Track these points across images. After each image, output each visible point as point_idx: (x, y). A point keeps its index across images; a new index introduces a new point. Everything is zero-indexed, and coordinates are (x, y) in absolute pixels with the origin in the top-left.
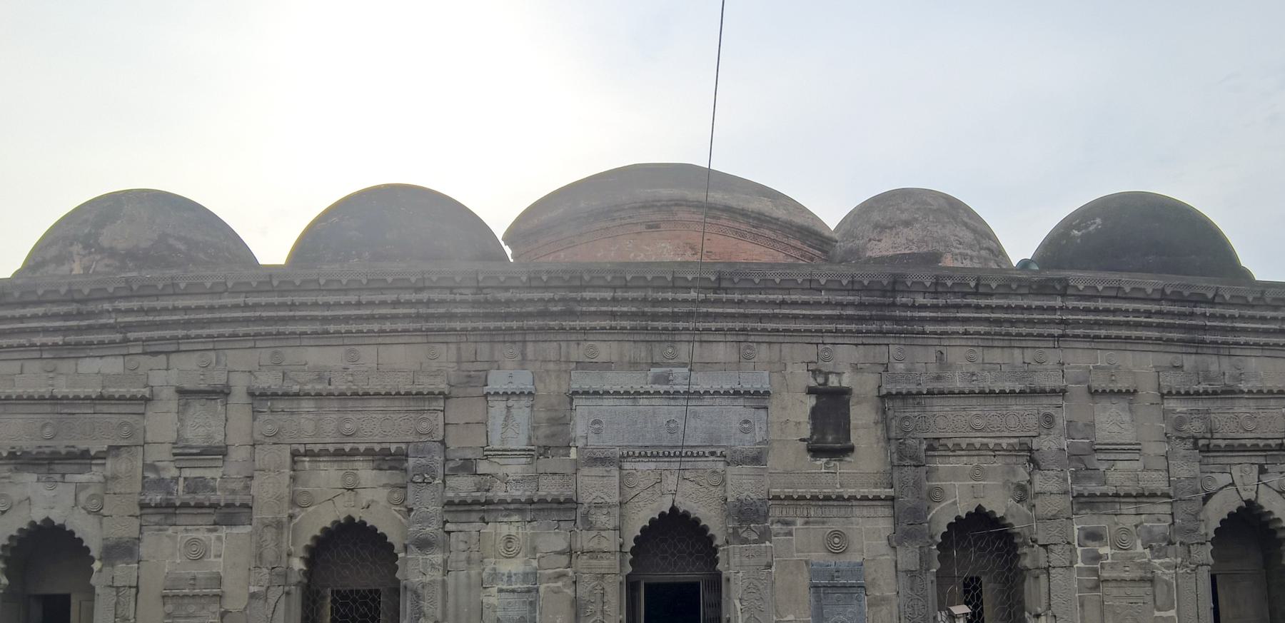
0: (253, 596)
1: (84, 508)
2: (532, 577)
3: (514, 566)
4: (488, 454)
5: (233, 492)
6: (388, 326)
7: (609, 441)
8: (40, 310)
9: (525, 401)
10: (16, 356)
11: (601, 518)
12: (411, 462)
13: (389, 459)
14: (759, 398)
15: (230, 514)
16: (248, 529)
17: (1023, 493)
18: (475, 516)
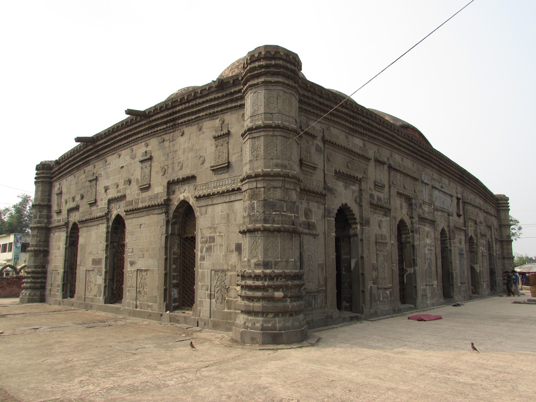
0: (392, 244)
1: (355, 201)
2: (430, 245)
3: (428, 241)
4: (424, 202)
5: (386, 203)
6: (407, 151)
7: (437, 204)
8: (346, 111)
9: (427, 187)
10: (339, 127)
11: (438, 228)
12: (413, 201)
13: (408, 199)
14: (451, 196)
15: (387, 211)
16: (388, 218)
17: (475, 231)
18: (423, 223)
